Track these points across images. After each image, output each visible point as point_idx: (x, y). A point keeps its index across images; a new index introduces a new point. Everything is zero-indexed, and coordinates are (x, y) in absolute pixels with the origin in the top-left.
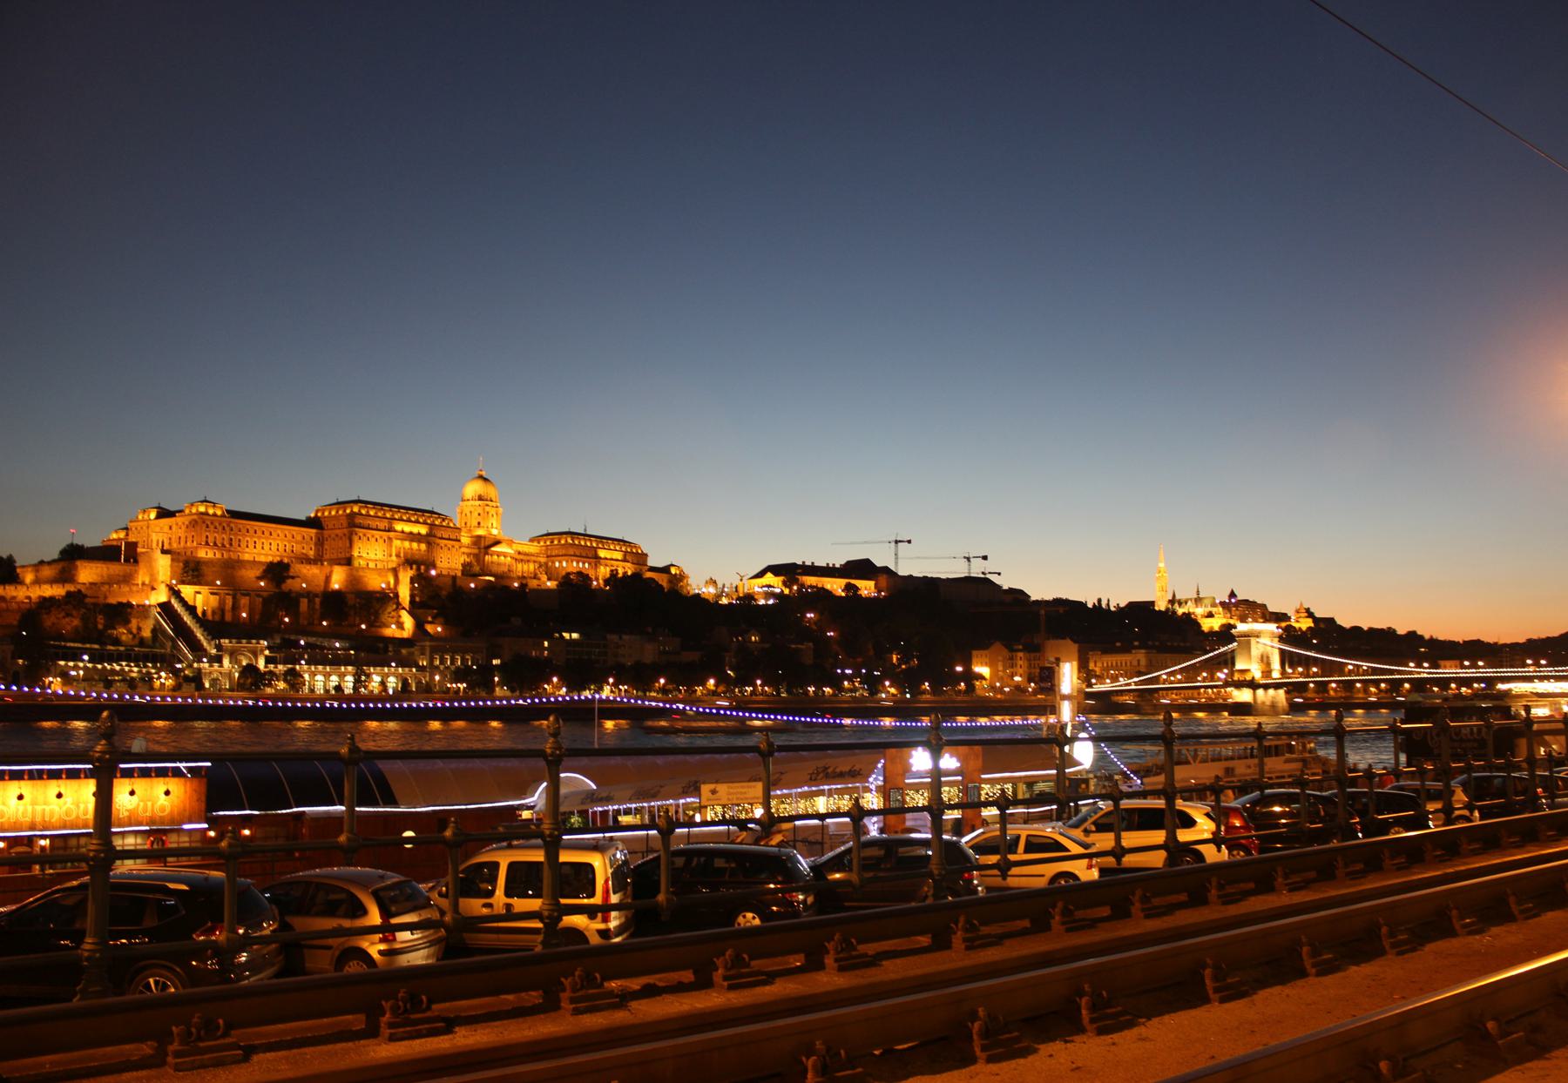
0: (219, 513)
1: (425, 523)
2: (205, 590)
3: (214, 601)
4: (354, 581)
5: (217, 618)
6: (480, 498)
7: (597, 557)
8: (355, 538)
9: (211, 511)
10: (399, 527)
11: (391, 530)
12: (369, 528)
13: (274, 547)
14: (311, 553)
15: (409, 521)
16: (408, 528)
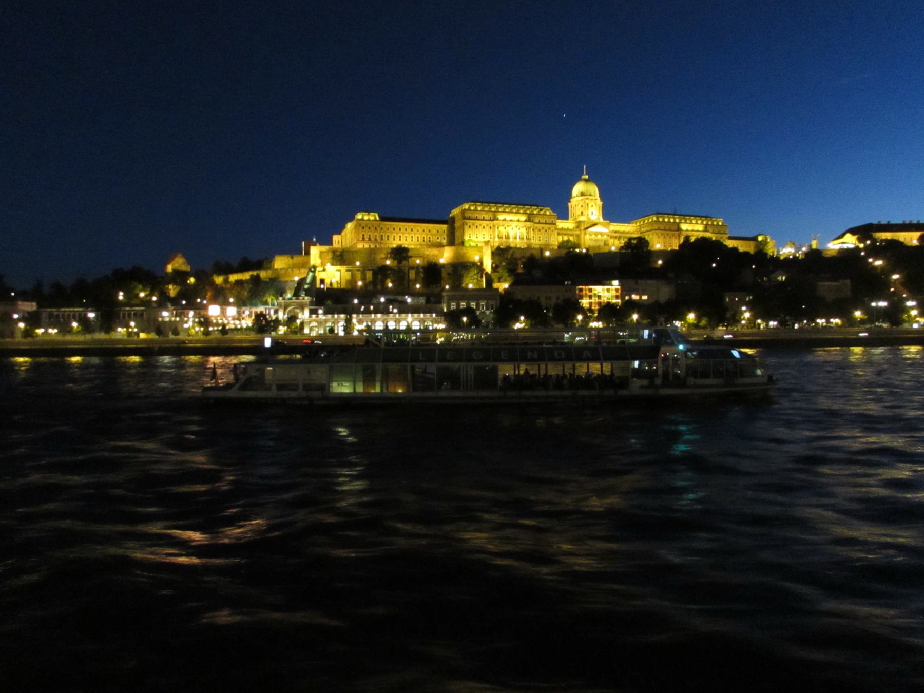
0: (372, 218)
1: (525, 213)
2: (343, 269)
3: (348, 276)
4: (457, 255)
5: (349, 287)
6: (582, 194)
7: (679, 229)
8: (466, 227)
9: (366, 218)
10: (501, 217)
11: (495, 219)
12: (477, 219)
13: (415, 239)
14: (445, 242)
15: (511, 212)
16: (509, 217)
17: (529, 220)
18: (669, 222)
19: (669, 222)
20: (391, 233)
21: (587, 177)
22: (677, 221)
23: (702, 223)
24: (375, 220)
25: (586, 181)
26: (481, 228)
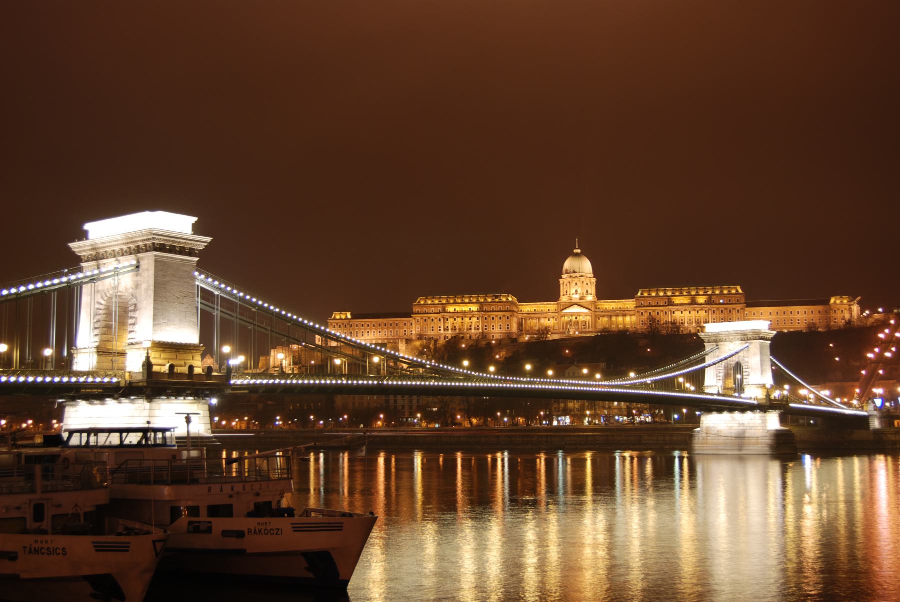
0: (343, 317)
6: (567, 273)
9: (338, 317)
10: (451, 309)
12: (426, 313)
15: (463, 303)
16: (458, 308)
17: (481, 310)
18: (657, 296)
19: (657, 296)
20: (360, 329)
21: (579, 251)
22: (669, 294)
23: (689, 294)
24: (346, 318)
25: (577, 255)
26: (429, 321)
